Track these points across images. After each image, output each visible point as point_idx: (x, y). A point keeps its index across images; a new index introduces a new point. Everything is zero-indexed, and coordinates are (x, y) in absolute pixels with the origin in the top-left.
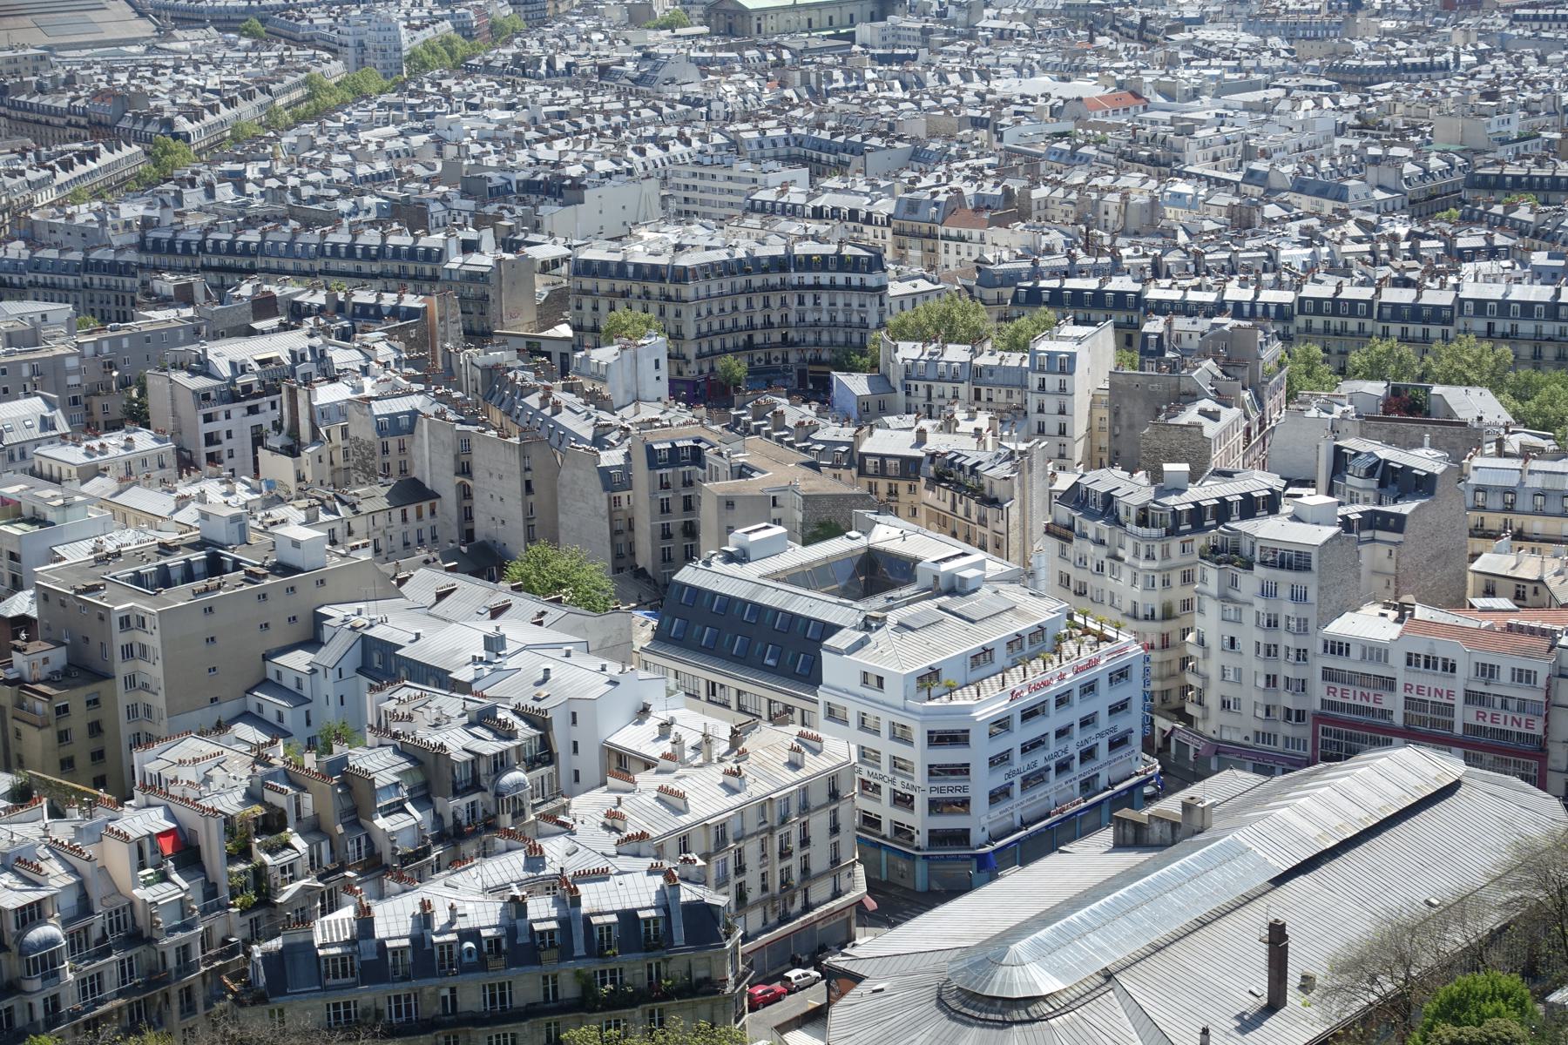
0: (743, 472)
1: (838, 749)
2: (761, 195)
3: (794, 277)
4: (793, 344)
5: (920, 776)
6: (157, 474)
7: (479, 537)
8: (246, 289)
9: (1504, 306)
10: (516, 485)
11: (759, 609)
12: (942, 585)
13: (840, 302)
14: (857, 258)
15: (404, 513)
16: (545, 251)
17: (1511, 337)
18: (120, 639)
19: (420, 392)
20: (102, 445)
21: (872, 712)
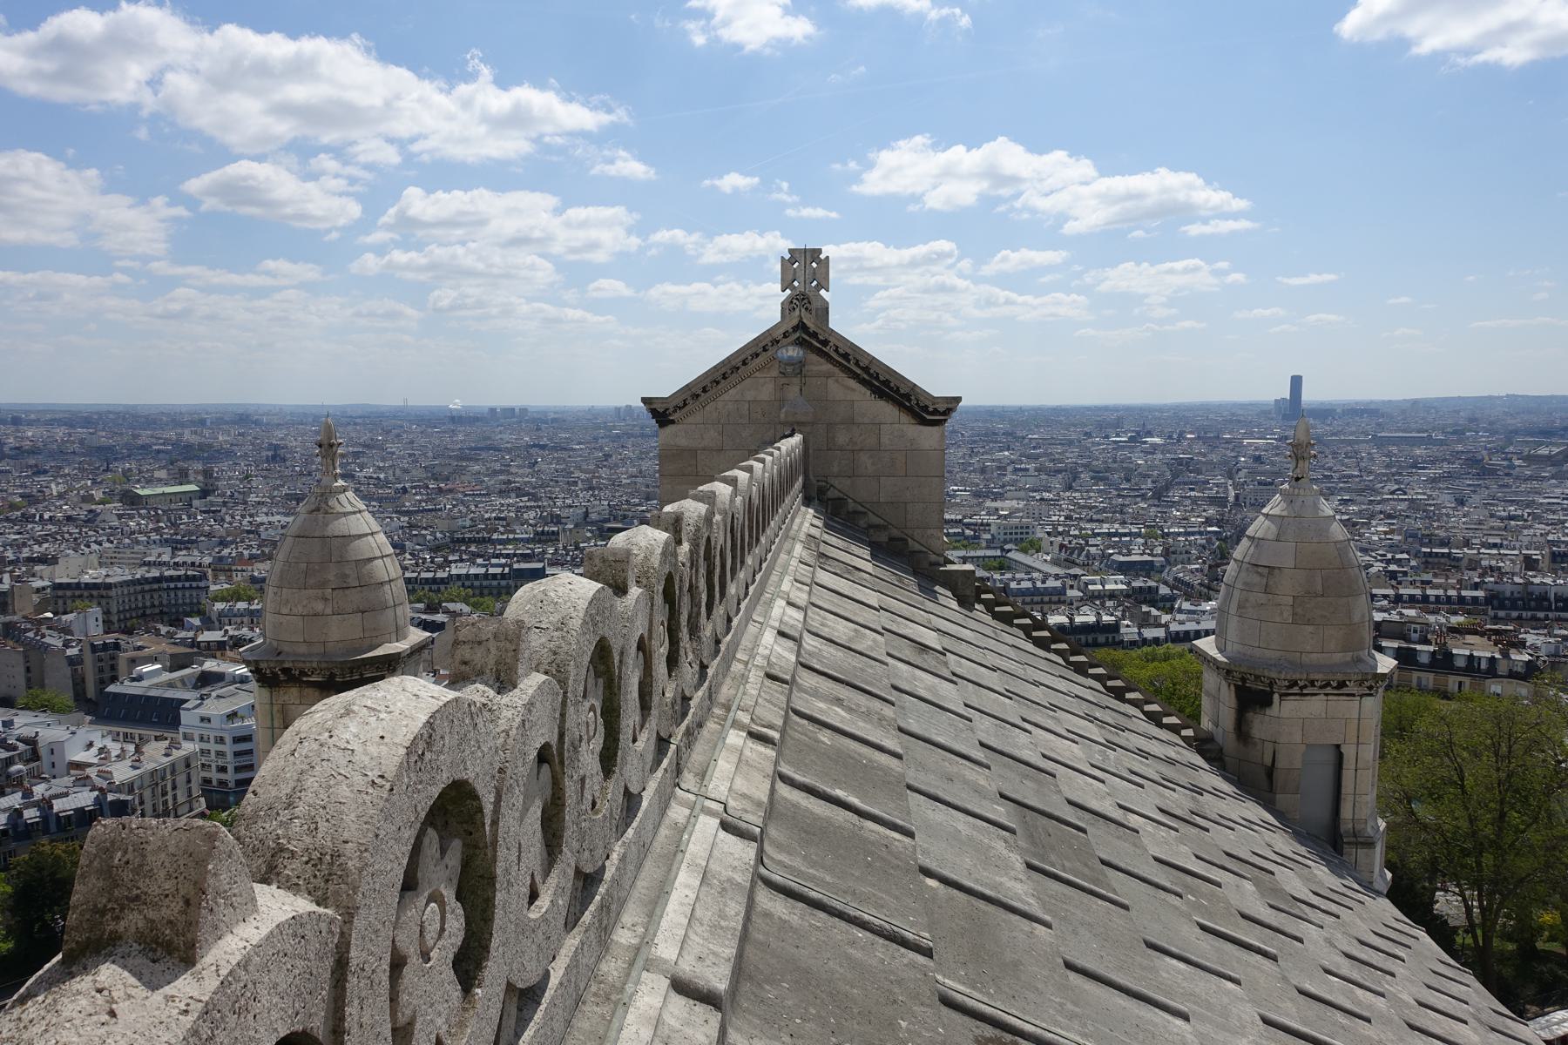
0: (140, 648)
1: (188, 747)
2: (147, 559)
4: (166, 613)
5: (230, 757)
9: (468, 576)
10: (22, 669)
11: (149, 698)
12: (237, 680)
16: (38, 584)
17: (472, 587)
21: (205, 733)
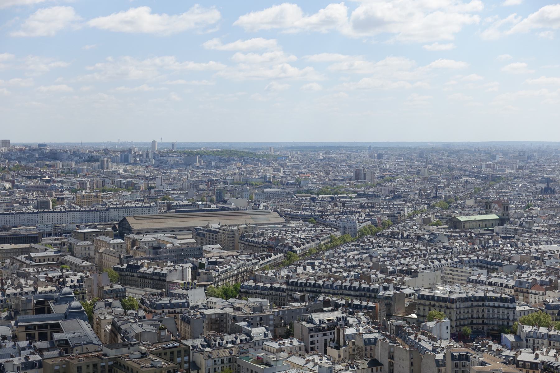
0: (483, 364)
2: (472, 277)
3: (486, 303)
4: (486, 324)
6: (299, 352)
8: (321, 298)
10: (408, 363)
13: (501, 312)
14: (507, 298)
15: (372, 369)
16: (408, 291)
19: (377, 332)
20: (284, 343)
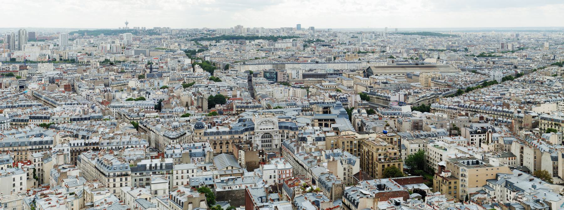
7: (524, 165)
18: (461, 173)
